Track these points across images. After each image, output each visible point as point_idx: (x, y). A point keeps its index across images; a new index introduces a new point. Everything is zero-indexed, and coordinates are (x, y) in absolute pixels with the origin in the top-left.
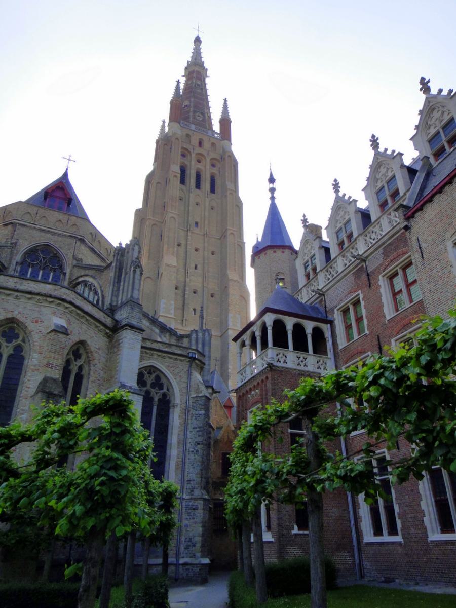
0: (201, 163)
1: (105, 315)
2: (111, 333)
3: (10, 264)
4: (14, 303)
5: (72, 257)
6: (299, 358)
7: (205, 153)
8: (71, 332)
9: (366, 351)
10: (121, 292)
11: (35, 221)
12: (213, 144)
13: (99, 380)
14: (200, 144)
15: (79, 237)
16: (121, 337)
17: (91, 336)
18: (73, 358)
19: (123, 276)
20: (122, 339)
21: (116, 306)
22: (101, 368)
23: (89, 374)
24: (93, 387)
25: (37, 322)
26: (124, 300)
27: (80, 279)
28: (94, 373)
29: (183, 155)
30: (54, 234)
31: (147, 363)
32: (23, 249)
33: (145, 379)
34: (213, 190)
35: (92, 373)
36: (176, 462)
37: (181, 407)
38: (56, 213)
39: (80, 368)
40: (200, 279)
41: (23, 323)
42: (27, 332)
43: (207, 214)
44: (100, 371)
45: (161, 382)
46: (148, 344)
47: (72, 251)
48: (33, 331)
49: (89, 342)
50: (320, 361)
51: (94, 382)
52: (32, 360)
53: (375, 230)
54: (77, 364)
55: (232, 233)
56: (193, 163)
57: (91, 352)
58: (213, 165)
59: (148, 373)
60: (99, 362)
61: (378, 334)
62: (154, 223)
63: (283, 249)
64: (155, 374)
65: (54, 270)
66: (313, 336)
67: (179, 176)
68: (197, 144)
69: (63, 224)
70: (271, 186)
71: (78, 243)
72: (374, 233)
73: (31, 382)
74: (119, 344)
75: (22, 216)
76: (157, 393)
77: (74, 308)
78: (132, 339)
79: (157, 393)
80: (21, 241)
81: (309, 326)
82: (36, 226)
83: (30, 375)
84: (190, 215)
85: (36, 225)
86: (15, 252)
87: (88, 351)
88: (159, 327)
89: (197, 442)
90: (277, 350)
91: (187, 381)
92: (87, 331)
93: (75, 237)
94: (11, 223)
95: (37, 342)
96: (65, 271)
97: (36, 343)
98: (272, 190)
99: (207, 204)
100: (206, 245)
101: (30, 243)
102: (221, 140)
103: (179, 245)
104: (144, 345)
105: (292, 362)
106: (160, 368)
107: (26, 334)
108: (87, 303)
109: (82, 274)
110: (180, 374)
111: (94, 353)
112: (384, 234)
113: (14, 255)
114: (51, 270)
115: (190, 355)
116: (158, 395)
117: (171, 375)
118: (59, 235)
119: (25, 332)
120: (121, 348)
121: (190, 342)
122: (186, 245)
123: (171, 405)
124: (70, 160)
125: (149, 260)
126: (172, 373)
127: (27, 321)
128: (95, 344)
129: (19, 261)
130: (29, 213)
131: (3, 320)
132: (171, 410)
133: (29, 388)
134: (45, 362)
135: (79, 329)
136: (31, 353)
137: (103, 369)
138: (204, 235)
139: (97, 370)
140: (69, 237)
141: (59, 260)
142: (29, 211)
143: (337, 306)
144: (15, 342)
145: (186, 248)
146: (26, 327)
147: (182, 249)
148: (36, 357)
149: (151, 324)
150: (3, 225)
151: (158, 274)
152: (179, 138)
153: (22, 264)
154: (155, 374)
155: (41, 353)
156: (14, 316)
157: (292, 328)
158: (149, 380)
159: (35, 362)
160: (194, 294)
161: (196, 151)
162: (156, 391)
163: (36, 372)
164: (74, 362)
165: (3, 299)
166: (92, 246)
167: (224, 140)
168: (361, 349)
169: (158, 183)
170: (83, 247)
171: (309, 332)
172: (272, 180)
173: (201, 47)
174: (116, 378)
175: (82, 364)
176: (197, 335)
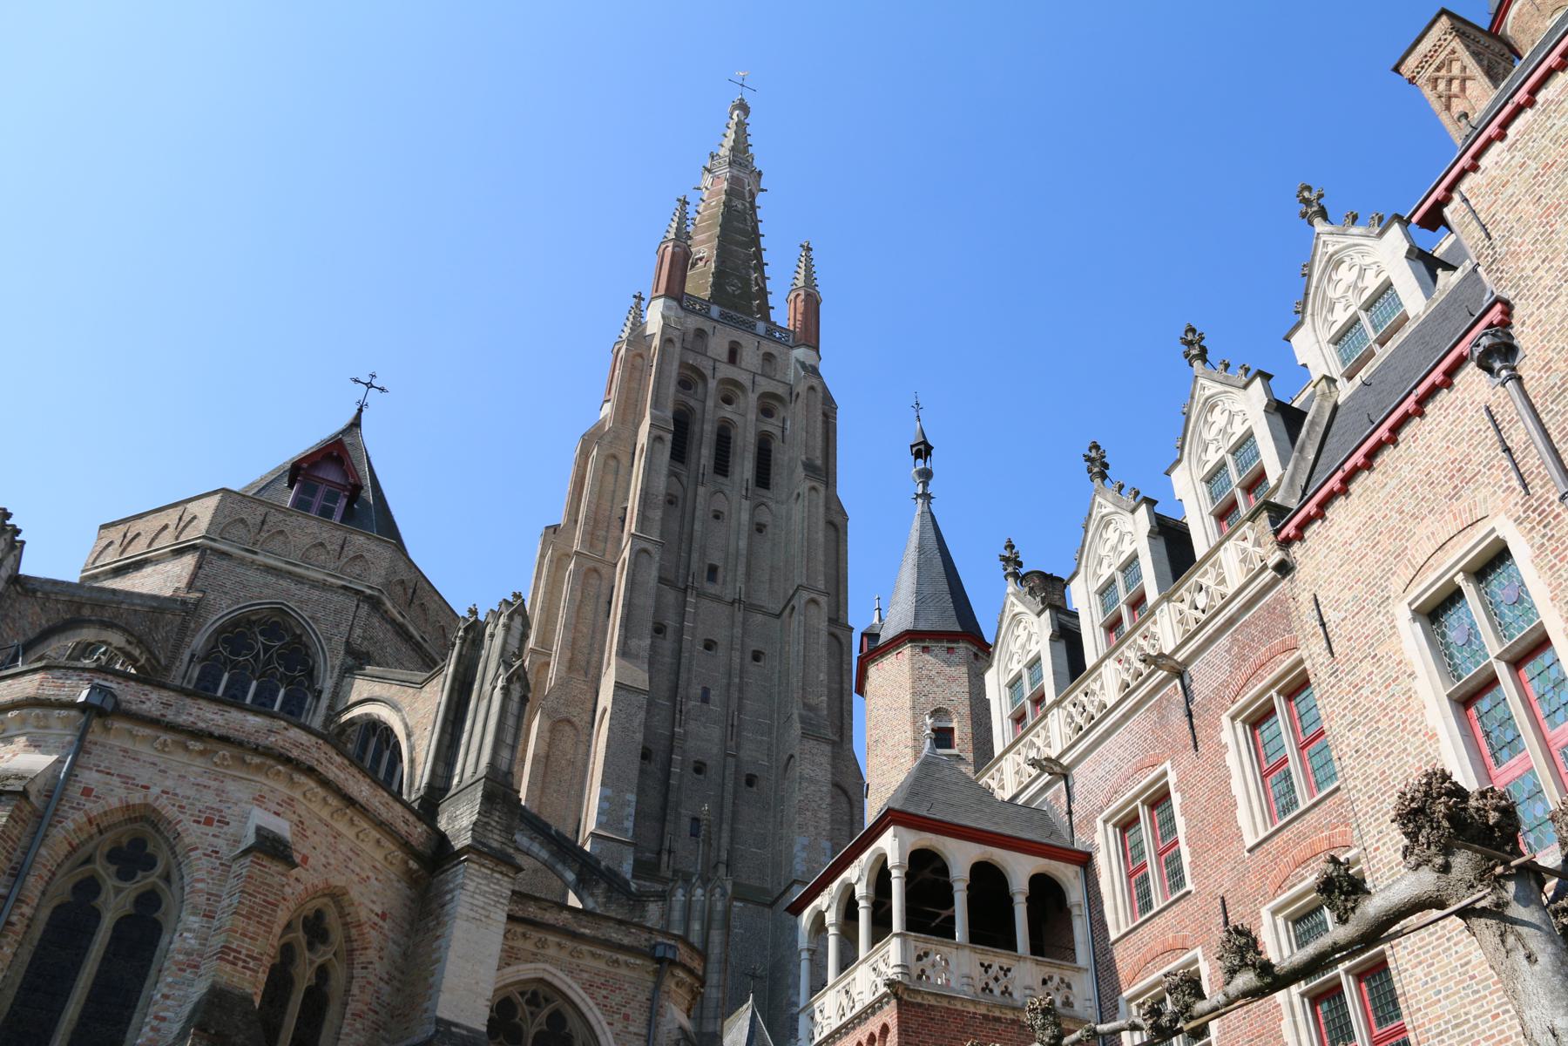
0: (734, 406)
4: (155, 764)
6: (987, 968)
7: (744, 378)
8: (305, 859)
9: (1188, 944)
12: (768, 357)
13: (376, 1012)
14: (733, 355)
15: (368, 591)
16: (451, 886)
17: (364, 876)
18: (304, 944)
20: (452, 891)
22: (386, 977)
23: (347, 991)
24: (357, 1031)
25: (209, 822)
28: (362, 989)
29: (684, 384)
30: (300, 580)
31: (526, 971)
34: (763, 477)
35: (355, 990)
39: (323, 972)
40: (716, 732)
41: (170, 823)
42: (178, 849)
43: (743, 544)
44: (382, 984)
46: (532, 911)
47: (344, 628)
48: (196, 848)
49: (354, 893)
50: (1051, 978)
51: (358, 1015)
52: (181, 935)
53: (1204, 582)
54: (314, 958)
55: (813, 601)
56: (710, 403)
58: (766, 412)
59: (528, 1002)
60: (381, 958)
61: (1221, 892)
62: (591, 564)
63: (949, 641)
65: (290, 681)
66: (1030, 900)
67: (669, 437)
68: (725, 356)
69: (328, 552)
70: (920, 464)
71: (365, 608)
72: (1203, 593)
73: (169, 1002)
74: (443, 906)
75: (224, 527)
78: (484, 894)
81: (1020, 870)
82: (255, 557)
83: (170, 980)
84: (696, 546)
85: (255, 553)
86: (192, 625)
87: (349, 919)
90: (919, 942)
91: (644, 1032)
92: (351, 859)
93: (358, 592)
95: (202, 880)
96: (318, 687)
97: (200, 886)
98: (926, 475)
99: (745, 517)
100: (738, 631)
101: (238, 603)
102: (791, 347)
103: (659, 629)
104: (520, 914)
106: (564, 988)
107: (174, 853)
110: (623, 1010)
111: (366, 929)
112: (1230, 591)
113: (189, 633)
114: (281, 680)
115: (659, 952)
117: (595, 1009)
118: (314, 584)
119: (172, 849)
120: (446, 918)
121: (666, 915)
122: (680, 631)
124: (370, 385)
125: (569, 668)
126: (603, 1007)
127: (182, 817)
128: (373, 902)
130: (242, 521)
131: (116, 809)
133: (164, 1019)
134: (217, 942)
135: (329, 853)
136: (183, 915)
138: (732, 603)
139: (372, 979)
140: (342, 591)
141: (307, 654)
142: (244, 516)
143: (1102, 811)
145: (680, 640)
146: (179, 834)
147: (667, 644)
148: (196, 926)
149: (552, 854)
151: (595, 711)
152: (676, 340)
153: (205, 659)
155: (209, 916)
156: (150, 800)
157: (967, 875)
159: (192, 942)
160: (695, 775)
161: (720, 375)
163: (188, 974)
164: (307, 954)
165: (125, 751)
167: (798, 346)
168: (1175, 938)
170: (376, 621)
171: (1019, 885)
172: (923, 450)
173: (746, 121)
174: (426, 1011)
175: (330, 960)
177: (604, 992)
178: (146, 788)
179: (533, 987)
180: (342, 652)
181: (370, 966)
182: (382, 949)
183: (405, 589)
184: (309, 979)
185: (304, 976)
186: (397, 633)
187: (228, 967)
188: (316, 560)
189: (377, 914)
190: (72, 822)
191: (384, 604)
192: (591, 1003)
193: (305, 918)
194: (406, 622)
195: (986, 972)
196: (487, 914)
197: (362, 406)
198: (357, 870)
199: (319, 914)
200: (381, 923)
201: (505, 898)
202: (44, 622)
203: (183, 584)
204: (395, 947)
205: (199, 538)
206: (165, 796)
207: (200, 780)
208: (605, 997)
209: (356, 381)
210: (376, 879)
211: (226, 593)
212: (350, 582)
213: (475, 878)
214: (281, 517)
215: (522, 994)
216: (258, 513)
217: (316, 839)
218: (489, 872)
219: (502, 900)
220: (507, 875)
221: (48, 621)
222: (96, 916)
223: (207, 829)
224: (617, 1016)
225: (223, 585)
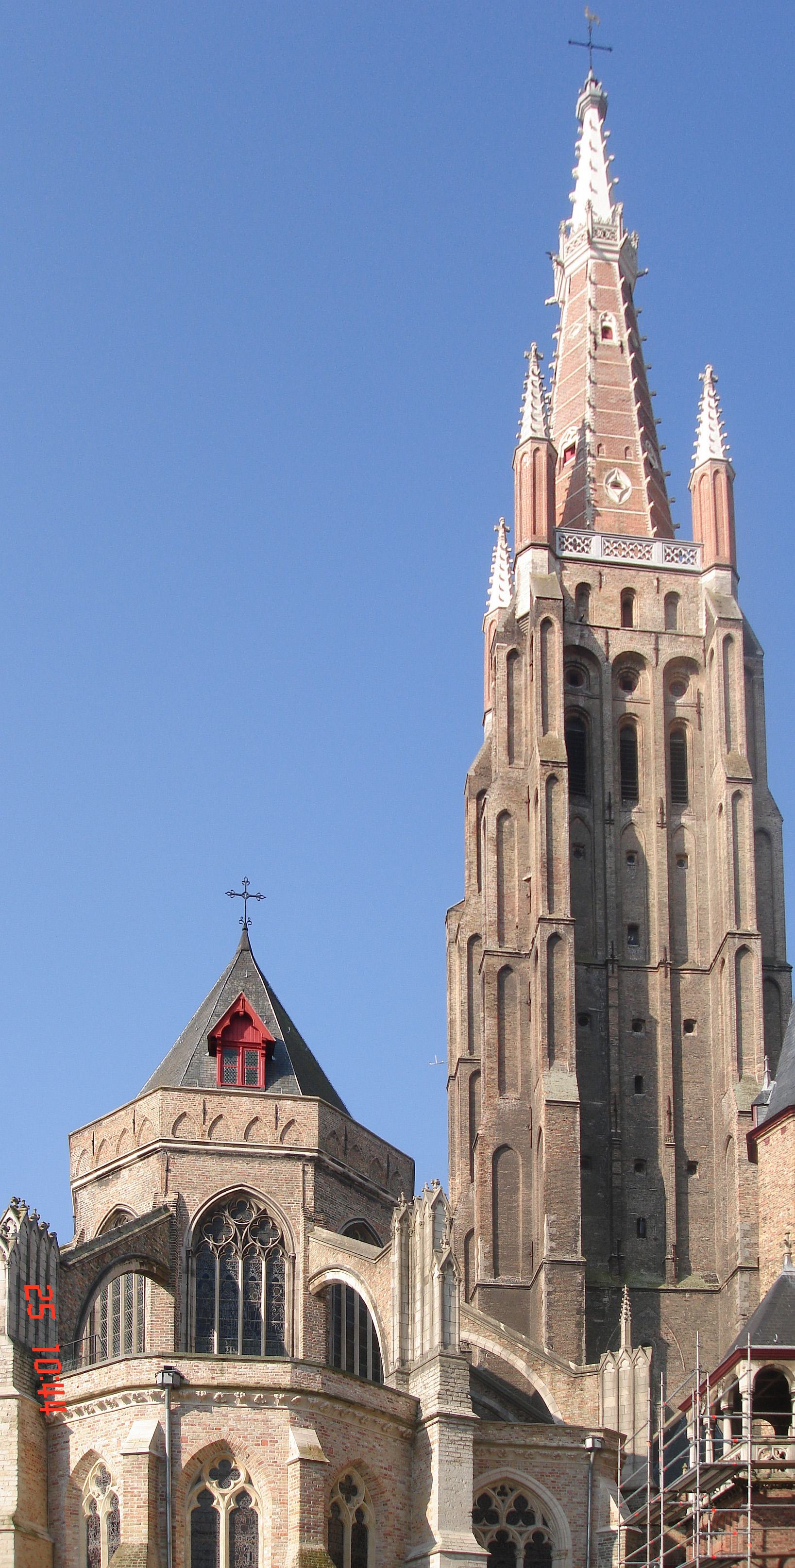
2: (409, 1431)
13: (399, 1530)
17: (371, 1446)
22: (400, 1506)
24: (390, 1545)
25: (264, 1443)
26: (427, 1347)
27: (330, 1276)
39: (360, 1513)
49: (367, 1460)
57: (375, 1479)
60: (394, 1495)
77: (327, 1403)
78: (453, 1442)
93: (299, 1158)
94: (155, 1151)
101: (204, 1195)
109: (332, 1262)
111: (381, 1480)
135: (345, 1440)
137: (404, 1505)
144: (235, 1485)
150: (139, 1157)
156: (224, 1437)
181: (388, 1503)
182: (393, 1489)
183: (337, 1139)
185: (349, 1519)
189: (385, 1469)
190: (185, 1458)
191: (324, 1161)
193: (340, 1483)
194: (346, 1170)
196: (459, 1455)
199: (349, 1478)
200: (389, 1473)
201: (469, 1441)
202: (87, 1282)
203: (159, 1188)
204: (402, 1485)
205: (157, 1142)
206: (232, 1432)
212: (291, 1149)
213: (446, 1433)
217: (334, 1434)
220: (468, 1425)
221: (89, 1280)
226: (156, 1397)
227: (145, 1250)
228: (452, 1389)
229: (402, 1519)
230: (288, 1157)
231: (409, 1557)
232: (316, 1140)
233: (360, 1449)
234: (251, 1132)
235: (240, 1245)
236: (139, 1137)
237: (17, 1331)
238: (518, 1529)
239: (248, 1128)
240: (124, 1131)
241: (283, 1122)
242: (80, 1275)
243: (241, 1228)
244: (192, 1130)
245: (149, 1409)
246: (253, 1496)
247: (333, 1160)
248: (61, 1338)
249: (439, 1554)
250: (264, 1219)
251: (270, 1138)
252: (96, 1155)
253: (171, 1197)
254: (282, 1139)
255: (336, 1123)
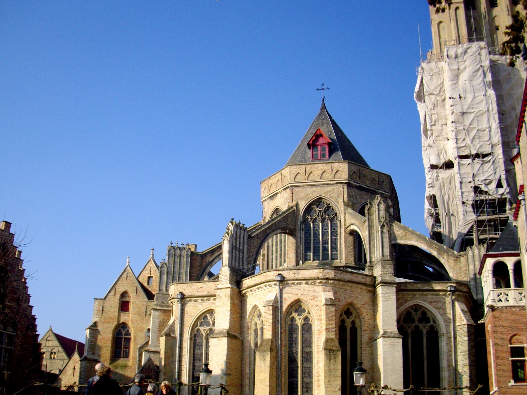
1: (363, 277)
3: (296, 225)
5: (342, 204)
6: (521, 294)
10: (376, 248)
11: (305, 180)
13: (370, 328)
17: (356, 296)
18: (346, 318)
19: (375, 235)
21: (374, 261)
22: (370, 318)
23: (361, 325)
25: (314, 299)
28: (364, 323)
32: (303, 208)
33: (412, 316)
35: (363, 324)
36: (449, 381)
37: (447, 336)
38: (320, 164)
44: (369, 321)
45: (427, 316)
47: (341, 197)
49: (355, 302)
54: (350, 320)
57: (359, 309)
59: (415, 311)
60: (367, 314)
64: (421, 310)
73: (318, 342)
76: (424, 327)
78: (388, 293)
79: (424, 327)
80: (299, 202)
87: (356, 308)
88: (437, 249)
89: (464, 364)
92: (351, 294)
94: (288, 187)
105: (513, 300)
108: (347, 274)
109: (352, 222)
111: (361, 309)
116: (426, 328)
121: (467, 260)
123: (439, 335)
124: (323, 89)
127: (307, 299)
128: (361, 302)
129: (301, 220)
132: (440, 339)
133: (319, 346)
135: (345, 295)
139: (367, 320)
140: (336, 185)
154: (421, 310)
156: (299, 297)
158: (417, 316)
162: (423, 325)
164: (348, 320)
166: (358, 185)
169: (440, 22)
175: (354, 319)
176: (473, 253)
177: (435, 304)
178: (297, 295)
179: (414, 307)
180: (343, 205)
182: (367, 312)
183: (356, 174)
184: (350, 325)
186: (359, 189)
187: (328, 332)
188: (325, 177)
189: (363, 304)
190: (285, 307)
191: (351, 183)
192: (432, 307)
194: (361, 185)
195: (521, 295)
196: (390, 298)
197: (323, 99)
198: (354, 296)
199: (348, 309)
200: (365, 306)
202: (259, 241)
203: (290, 200)
204: (370, 310)
207: (308, 289)
208: (436, 305)
209: (318, 90)
210: (360, 296)
211: (303, 199)
212: (338, 180)
214: (309, 166)
215: (412, 309)
216: (303, 169)
217: (341, 293)
218: (388, 287)
219: (393, 293)
222: (297, 325)
223: (313, 301)
224: (440, 310)
225: (301, 197)
226: (275, 284)
227: (283, 225)
228: (386, 272)
229: (371, 324)
230: (337, 183)
231: (374, 339)
232: (347, 176)
233: (351, 298)
234: (323, 176)
235: (320, 218)
236: (283, 182)
237: (232, 264)
238: (423, 325)
239: (322, 175)
240: (278, 180)
241: (334, 171)
242: (257, 239)
243: (320, 211)
244: (301, 178)
245: (273, 289)
246: (311, 319)
247: (355, 182)
248: (249, 263)
249: (382, 338)
250: (329, 207)
251: (330, 177)
252: (269, 190)
253: (294, 203)
254: (334, 177)
255: (355, 168)
